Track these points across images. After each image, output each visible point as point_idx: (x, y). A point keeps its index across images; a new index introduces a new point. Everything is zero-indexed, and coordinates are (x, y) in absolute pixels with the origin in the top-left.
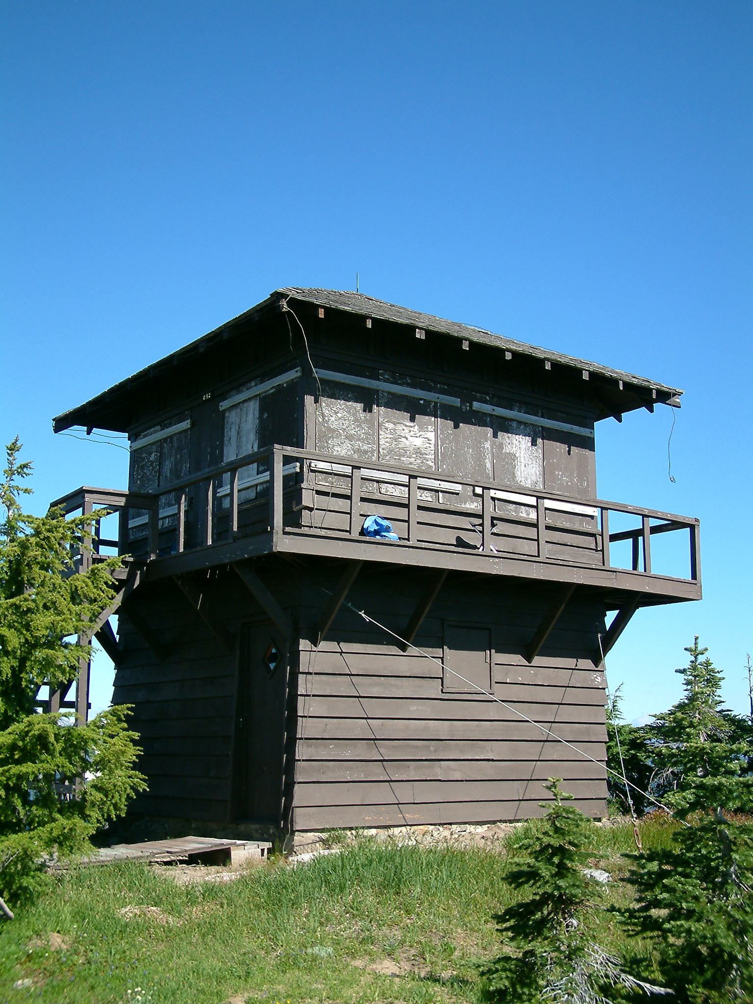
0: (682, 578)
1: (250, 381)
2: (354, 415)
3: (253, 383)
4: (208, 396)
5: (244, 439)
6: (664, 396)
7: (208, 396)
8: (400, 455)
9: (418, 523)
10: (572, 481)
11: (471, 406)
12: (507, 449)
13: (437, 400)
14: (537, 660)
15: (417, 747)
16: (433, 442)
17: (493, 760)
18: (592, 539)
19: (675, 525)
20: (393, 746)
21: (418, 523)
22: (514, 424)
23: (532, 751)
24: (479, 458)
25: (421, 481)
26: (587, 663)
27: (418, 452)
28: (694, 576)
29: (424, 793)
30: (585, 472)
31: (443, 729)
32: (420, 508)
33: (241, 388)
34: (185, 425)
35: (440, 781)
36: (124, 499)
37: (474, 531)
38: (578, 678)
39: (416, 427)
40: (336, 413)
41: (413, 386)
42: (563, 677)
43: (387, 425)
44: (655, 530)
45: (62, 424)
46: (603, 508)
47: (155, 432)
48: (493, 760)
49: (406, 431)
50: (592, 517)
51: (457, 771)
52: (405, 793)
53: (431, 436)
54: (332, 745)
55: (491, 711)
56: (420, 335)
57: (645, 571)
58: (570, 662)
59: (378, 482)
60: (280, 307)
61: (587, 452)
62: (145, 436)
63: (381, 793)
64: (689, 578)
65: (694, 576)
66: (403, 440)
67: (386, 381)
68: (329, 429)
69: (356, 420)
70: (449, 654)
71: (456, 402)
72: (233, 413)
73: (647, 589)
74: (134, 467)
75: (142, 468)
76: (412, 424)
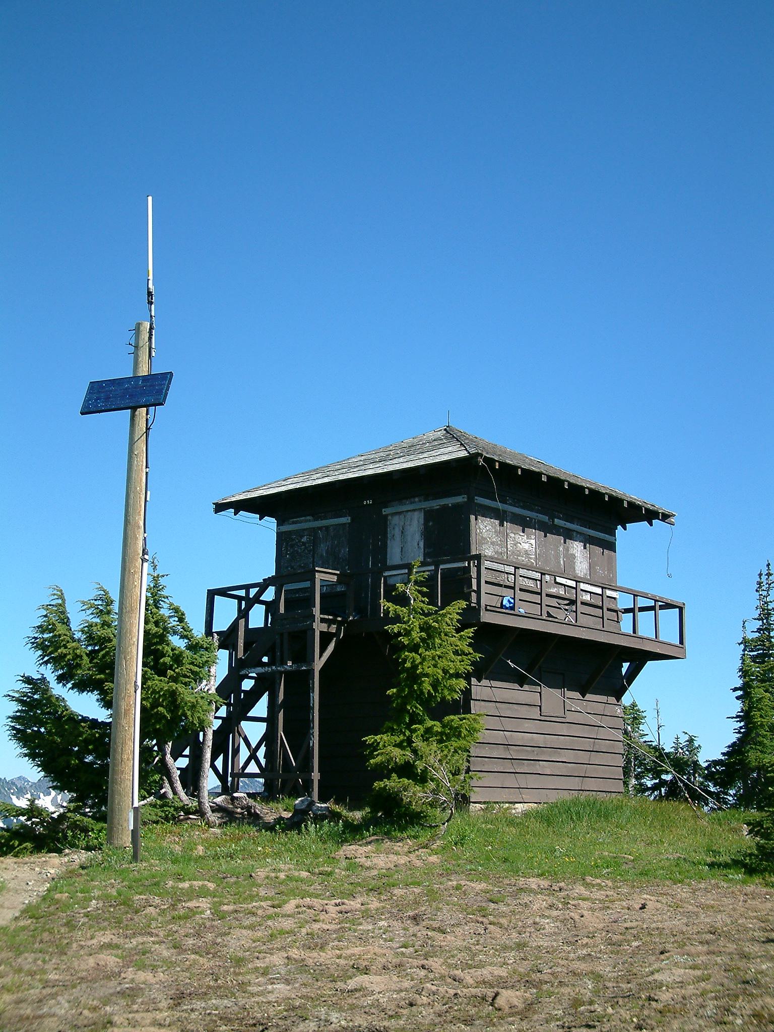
0: (673, 642)
1: (414, 497)
2: (495, 528)
3: (417, 499)
4: (370, 502)
5: (409, 538)
6: (665, 517)
7: (370, 502)
8: (518, 556)
9: (486, 593)
10: (604, 573)
11: (553, 521)
12: (571, 551)
13: (536, 518)
14: (589, 697)
15: (527, 751)
16: (534, 546)
17: (565, 762)
18: (615, 614)
19: (668, 606)
20: (518, 750)
21: (486, 593)
22: (575, 534)
23: (583, 757)
24: (557, 557)
25: (522, 572)
26: (612, 700)
27: (527, 553)
28: (681, 642)
29: (533, 781)
30: (611, 566)
31: (540, 740)
32: (521, 590)
33: (404, 501)
34: (346, 520)
35: (539, 774)
36: (336, 577)
37: (560, 608)
38: (609, 710)
39: (525, 536)
40: (486, 527)
41: (523, 508)
42: (599, 708)
43: (511, 535)
44: (661, 608)
45: (220, 507)
46: (635, 595)
47: (306, 521)
48: (565, 762)
49: (520, 539)
50: (615, 598)
51: (547, 768)
52: (522, 781)
53: (533, 542)
54: (487, 747)
55: (564, 729)
56: (544, 479)
57: (656, 638)
58: (603, 698)
59: (507, 573)
60: (478, 462)
61: (613, 553)
62: (294, 523)
63: (510, 781)
64: (677, 643)
65: (681, 642)
66: (519, 545)
67: (511, 505)
68: (482, 537)
69: (496, 532)
70: (546, 690)
71: (545, 518)
72: (396, 518)
73: (658, 651)
74: (282, 544)
75: (292, 546)
76: (523, 534)
